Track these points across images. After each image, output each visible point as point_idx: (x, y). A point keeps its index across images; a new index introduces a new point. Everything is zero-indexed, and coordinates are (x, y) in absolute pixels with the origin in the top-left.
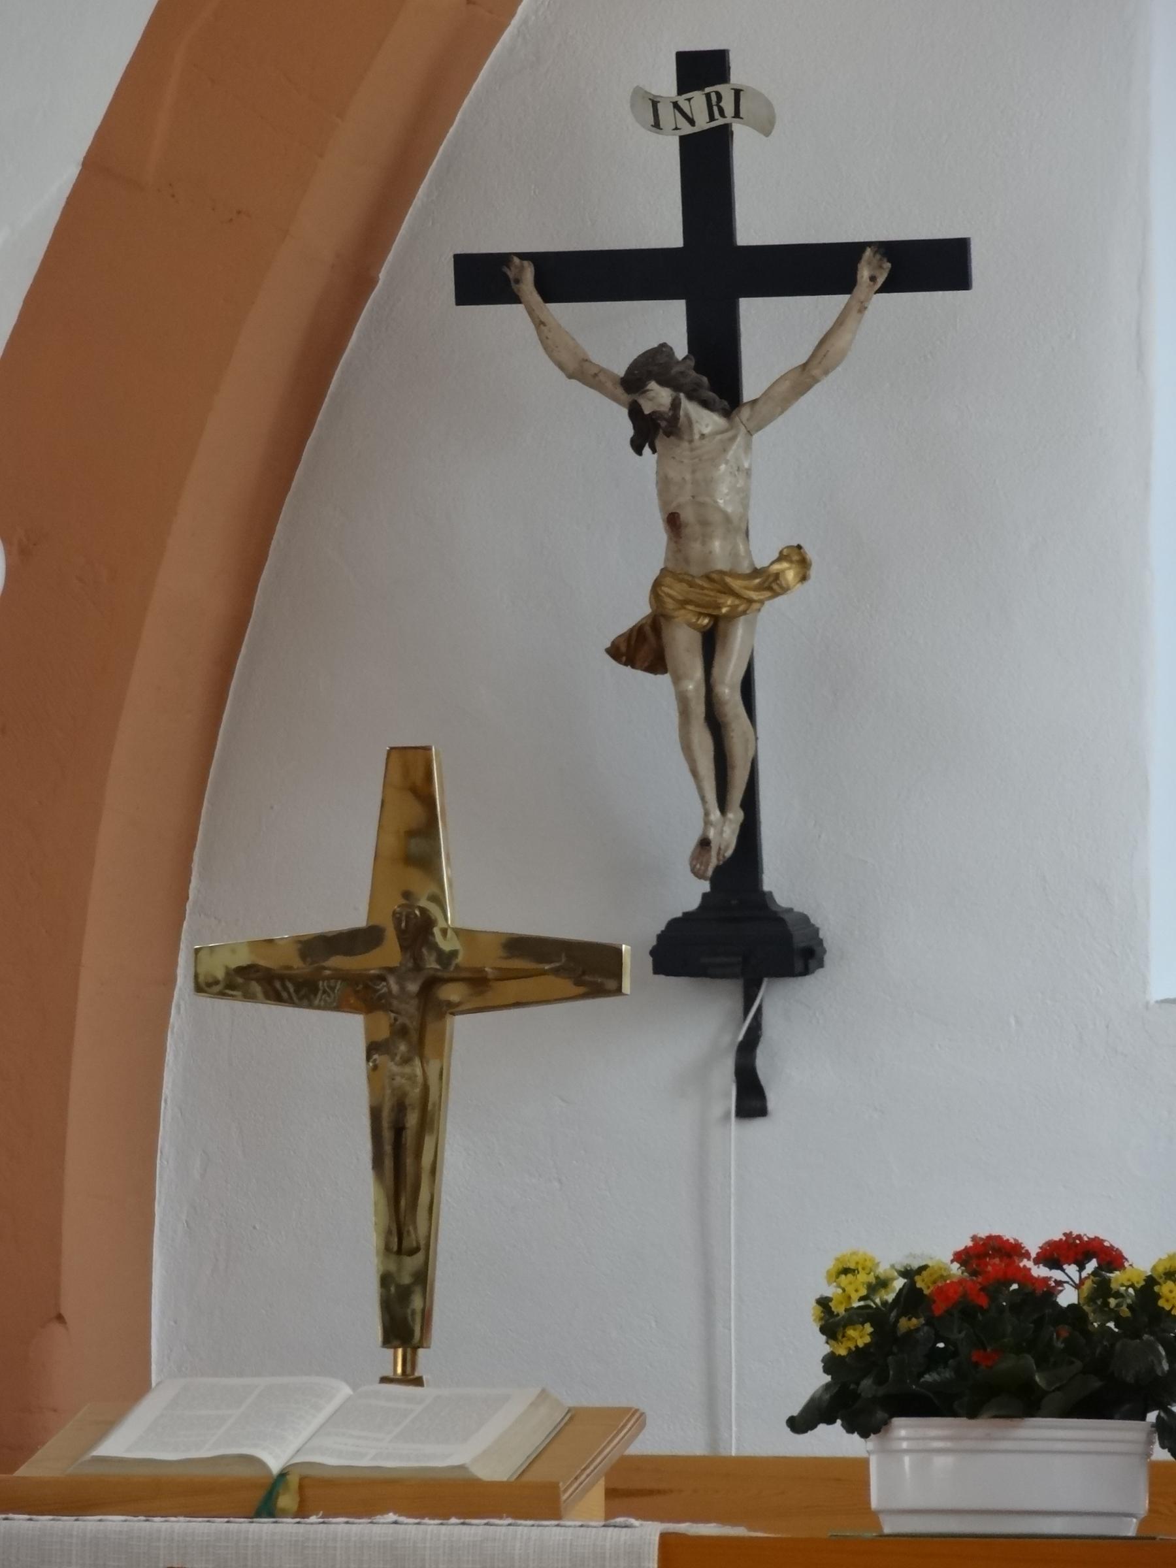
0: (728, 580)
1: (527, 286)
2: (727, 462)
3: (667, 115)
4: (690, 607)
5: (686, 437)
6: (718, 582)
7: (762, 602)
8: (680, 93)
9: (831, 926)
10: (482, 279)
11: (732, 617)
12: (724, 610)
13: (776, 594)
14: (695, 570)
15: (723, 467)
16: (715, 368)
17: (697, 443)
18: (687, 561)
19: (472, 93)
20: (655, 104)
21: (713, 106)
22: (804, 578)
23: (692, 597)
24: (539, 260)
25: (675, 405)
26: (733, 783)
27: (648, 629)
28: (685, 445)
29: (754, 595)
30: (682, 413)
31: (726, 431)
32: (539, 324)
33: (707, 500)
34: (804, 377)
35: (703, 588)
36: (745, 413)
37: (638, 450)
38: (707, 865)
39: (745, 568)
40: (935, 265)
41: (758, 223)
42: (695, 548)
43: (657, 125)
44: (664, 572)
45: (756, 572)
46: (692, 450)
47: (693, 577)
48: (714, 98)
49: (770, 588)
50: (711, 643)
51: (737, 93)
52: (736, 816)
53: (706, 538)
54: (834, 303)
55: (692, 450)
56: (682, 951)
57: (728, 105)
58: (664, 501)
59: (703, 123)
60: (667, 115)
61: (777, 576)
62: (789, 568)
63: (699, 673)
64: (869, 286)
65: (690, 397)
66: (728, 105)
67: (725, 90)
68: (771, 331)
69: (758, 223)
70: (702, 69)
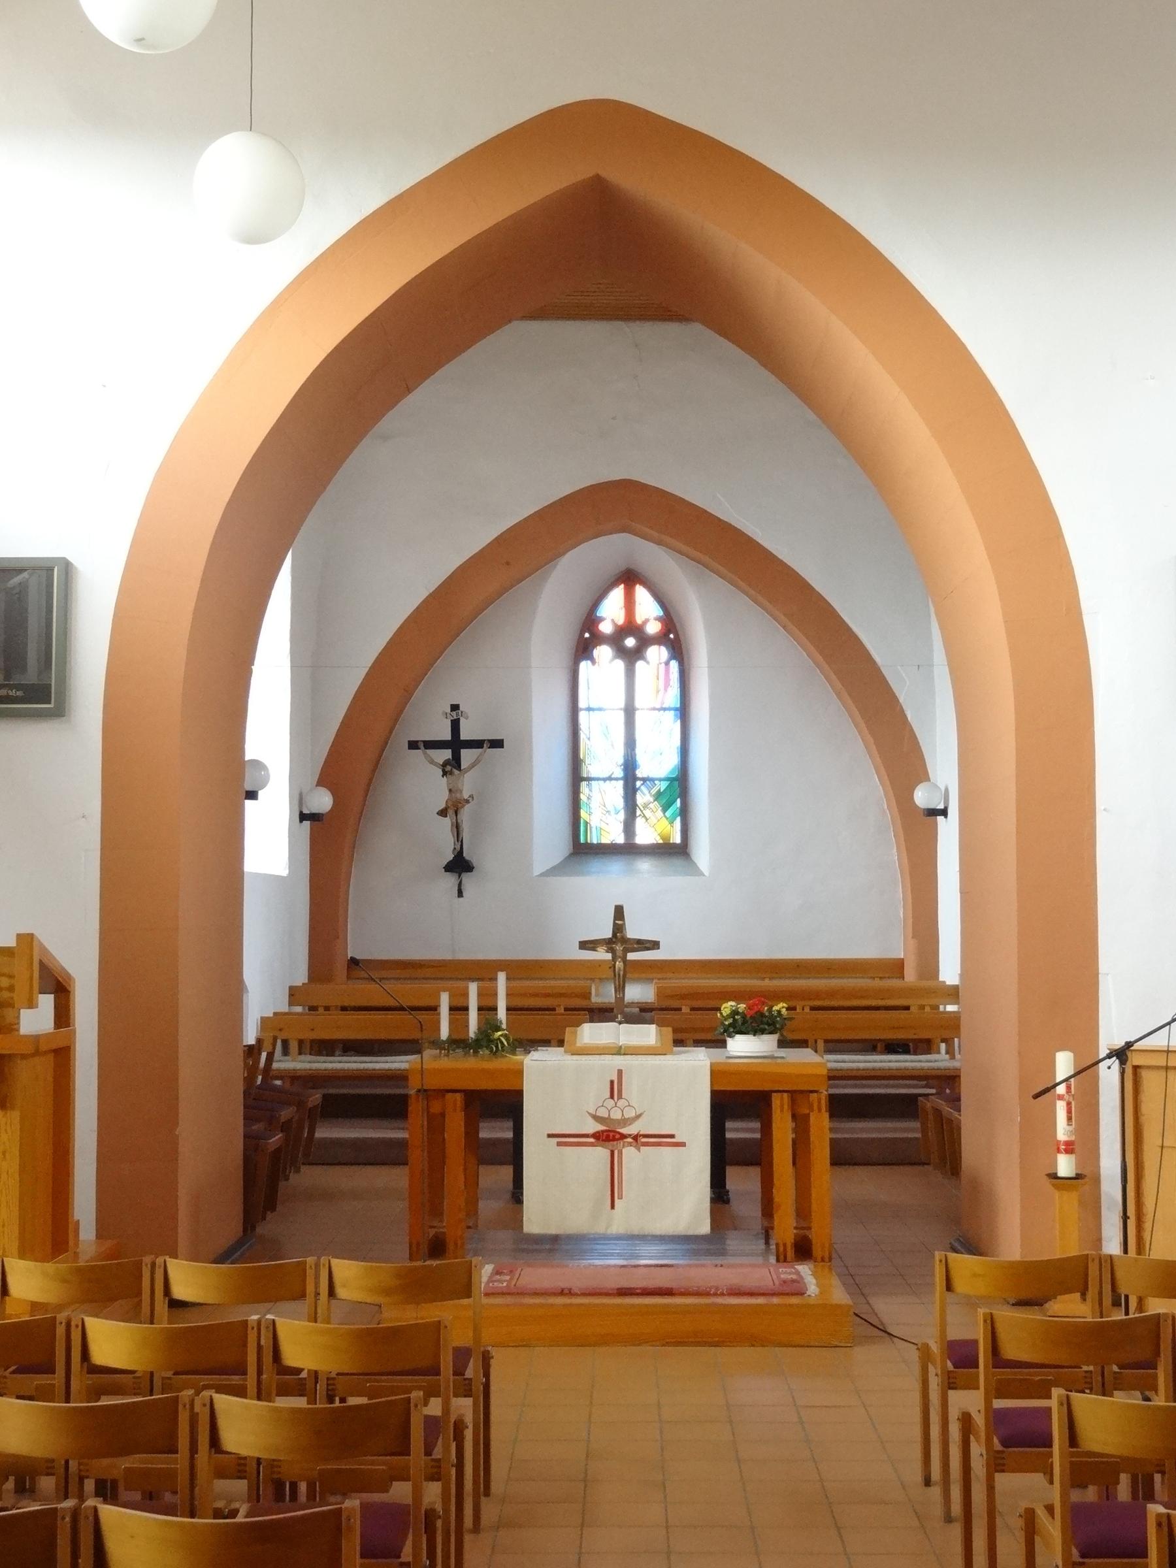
1: (422, 745)
9: (475, 863)
10: (413, 745)
16: (456, 761)
24: (424, 742)
32: (425, 754)
34: (473, 766)
40: (497, 744)
54: (480, 750)
56: (449, 868)
68: (467, 755)
70: (455, 708)
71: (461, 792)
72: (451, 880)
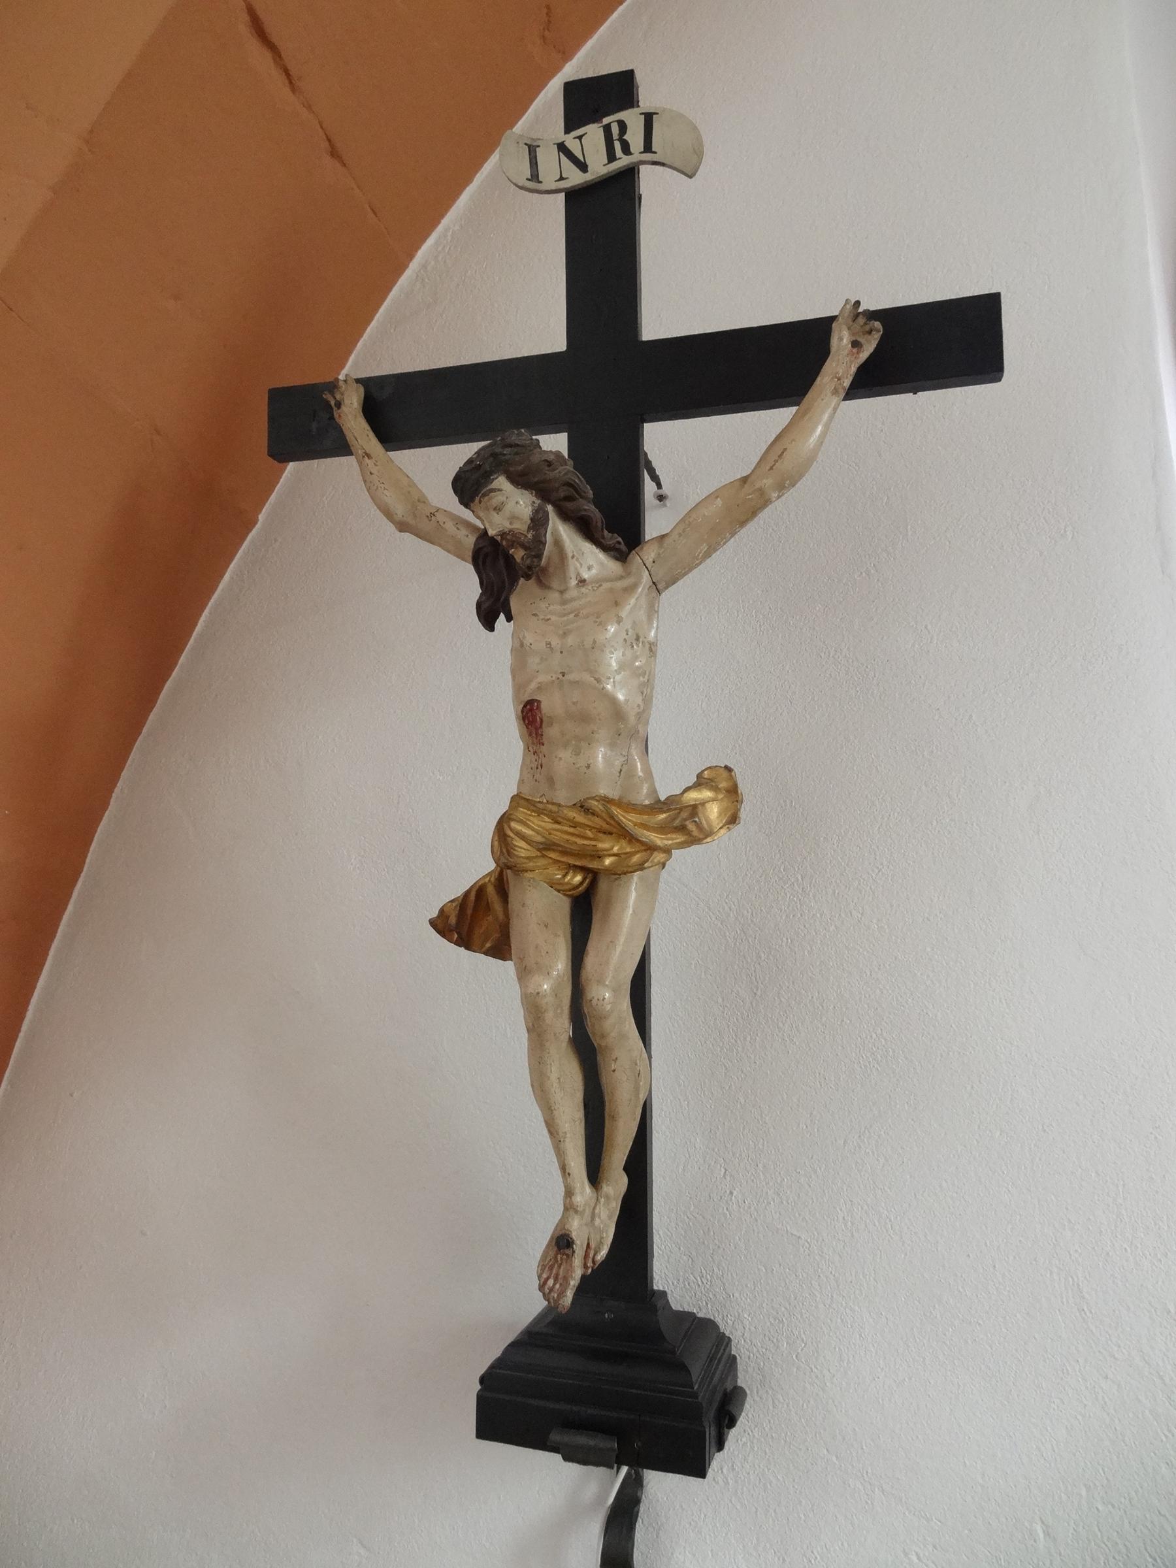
0: (616, 811)
2: (619, 621)
3: (549, 161)
4: (553, 855)
5: (555, 584)
6: (603, 816)
7: (668, 851)
8: (568, 130)
11: (620, 873)
12: (608, 861)
13: (693, 841)
14: (562, 796)
15: (612, 629)
17: (573, 593)
18: (551, 781)
19: (365, 336)
20: (532, 150)
21: (614, 143)
22: (733, 820)
23: (557, 837)
25: (538, 522)
26: (614, 1145)
27: (491, 890)
28: (554, 596)
29: (657, 839)
30: (549, 537)
31: (621, 578)
33: (587, 678)
34: (744, 502)
35: (575, 825)
36: (649, 553)
37: (488, 621)
38: (566, 1279)
39: (643, 797)
40: (944, 344)
41: (670, 309)
42: (563, 760)
43: (535, 176)
44: (517, 800)
45: (659, 806)
46: (564, 602)
47: (559, 805)
48: (615, 129)
49: (682, 829)
50: (583, 913)
51: (649, 118)
52: (617, 1184)
53: (584, 742)
55: (564, 602)
57: (635, 137)
58: (518, 688)
59: (599, 167)
60: (549, 161)
61: (694, 809)
62: (713, 800)
63: (561, 965)
64: (851, 354)
65: (565, 516)
66: (635, 137)
67: (633, 118)
68: (689, 455)
69: (670, 309)
71: (627, 728)
72: (550, 1492)
